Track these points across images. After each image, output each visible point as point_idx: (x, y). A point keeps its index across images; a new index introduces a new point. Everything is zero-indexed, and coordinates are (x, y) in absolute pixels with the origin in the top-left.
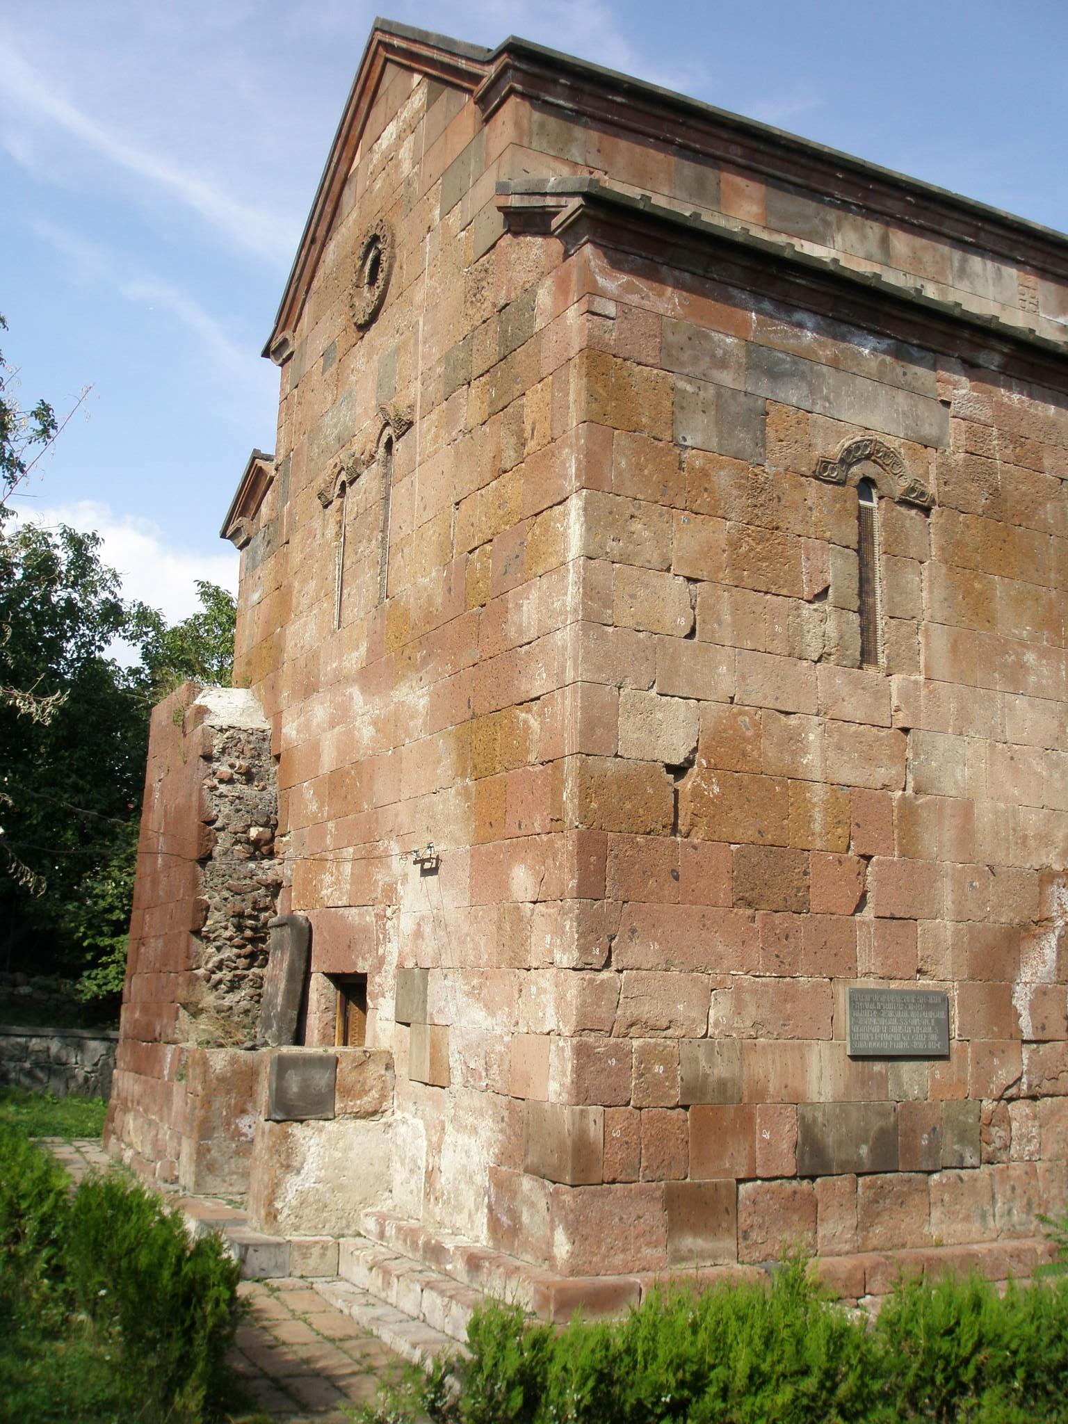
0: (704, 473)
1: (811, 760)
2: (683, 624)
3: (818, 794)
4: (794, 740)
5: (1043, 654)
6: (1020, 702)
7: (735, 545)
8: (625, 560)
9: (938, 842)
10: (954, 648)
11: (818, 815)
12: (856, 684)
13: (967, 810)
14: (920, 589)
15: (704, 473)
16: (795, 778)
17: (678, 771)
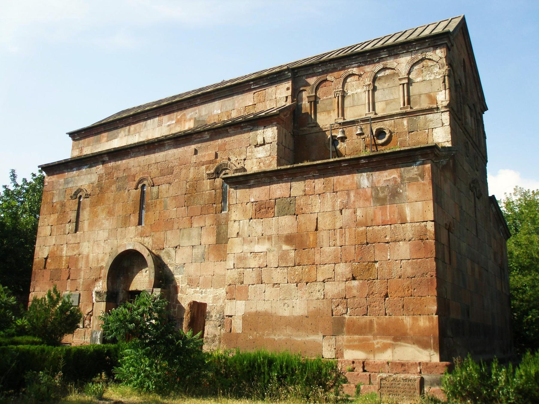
0: (56, 206)
1: (64, 253)
2: (49, 234)
3: (65, 258)
4: (62, 250)
5: (107, 220)
6: (101, 232)
7: (58, 217)
8: (43, 226)
9: (82, 264)
10: (89, 224)
11: (64, 262)
12: (73, 236)
13: (88, 256)
14: (85, 214)
15: (56, 206)
16: (61, 257)
17: (46, 259)
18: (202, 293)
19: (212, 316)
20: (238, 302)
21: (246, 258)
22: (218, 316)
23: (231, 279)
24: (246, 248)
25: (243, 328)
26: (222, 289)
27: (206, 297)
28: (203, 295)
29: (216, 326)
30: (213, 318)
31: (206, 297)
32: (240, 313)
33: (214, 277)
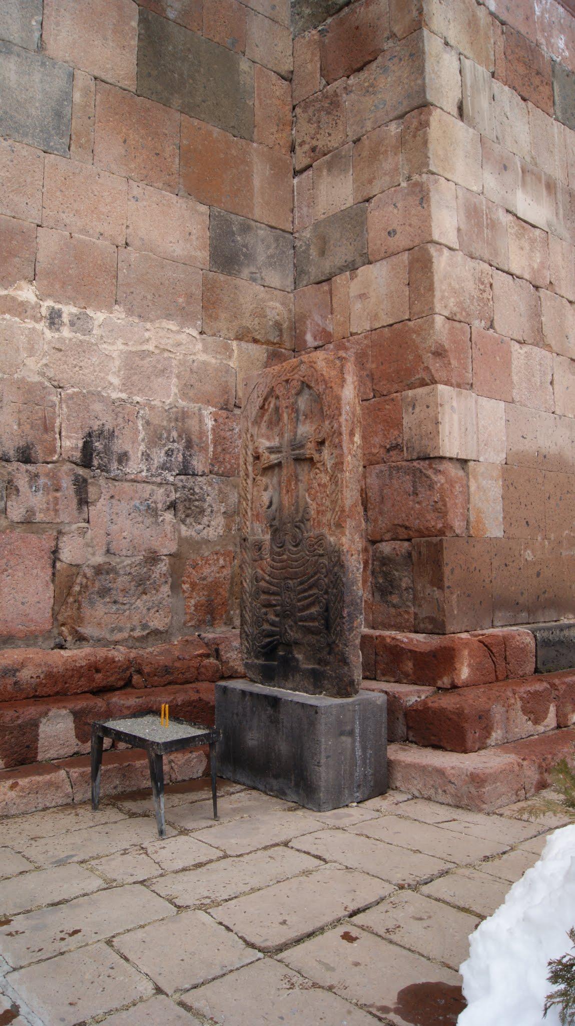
18: (54, 319)
19: (123, 458)
20: (483, 401)
21: (493, 225)
22: (159, 456)
23: (455, 292)
24: (490, 181)
25: (508, 519)
26: (172, 326)
27: (83, 348)
28: (66, 332)
29: (152, 511)
30: (135, 466)
31: (83, 348)
32: (493, 456)
33: (133, 255)
